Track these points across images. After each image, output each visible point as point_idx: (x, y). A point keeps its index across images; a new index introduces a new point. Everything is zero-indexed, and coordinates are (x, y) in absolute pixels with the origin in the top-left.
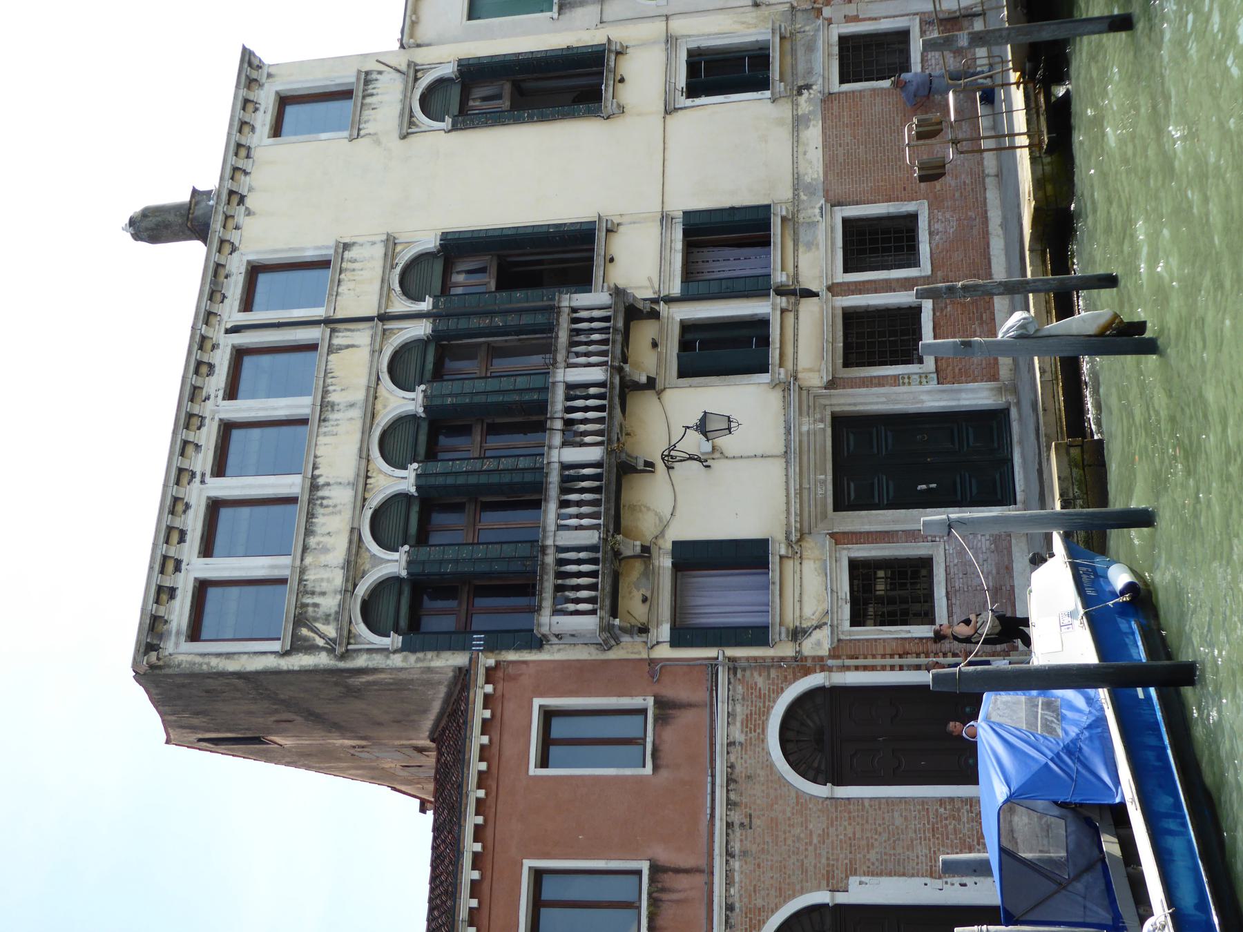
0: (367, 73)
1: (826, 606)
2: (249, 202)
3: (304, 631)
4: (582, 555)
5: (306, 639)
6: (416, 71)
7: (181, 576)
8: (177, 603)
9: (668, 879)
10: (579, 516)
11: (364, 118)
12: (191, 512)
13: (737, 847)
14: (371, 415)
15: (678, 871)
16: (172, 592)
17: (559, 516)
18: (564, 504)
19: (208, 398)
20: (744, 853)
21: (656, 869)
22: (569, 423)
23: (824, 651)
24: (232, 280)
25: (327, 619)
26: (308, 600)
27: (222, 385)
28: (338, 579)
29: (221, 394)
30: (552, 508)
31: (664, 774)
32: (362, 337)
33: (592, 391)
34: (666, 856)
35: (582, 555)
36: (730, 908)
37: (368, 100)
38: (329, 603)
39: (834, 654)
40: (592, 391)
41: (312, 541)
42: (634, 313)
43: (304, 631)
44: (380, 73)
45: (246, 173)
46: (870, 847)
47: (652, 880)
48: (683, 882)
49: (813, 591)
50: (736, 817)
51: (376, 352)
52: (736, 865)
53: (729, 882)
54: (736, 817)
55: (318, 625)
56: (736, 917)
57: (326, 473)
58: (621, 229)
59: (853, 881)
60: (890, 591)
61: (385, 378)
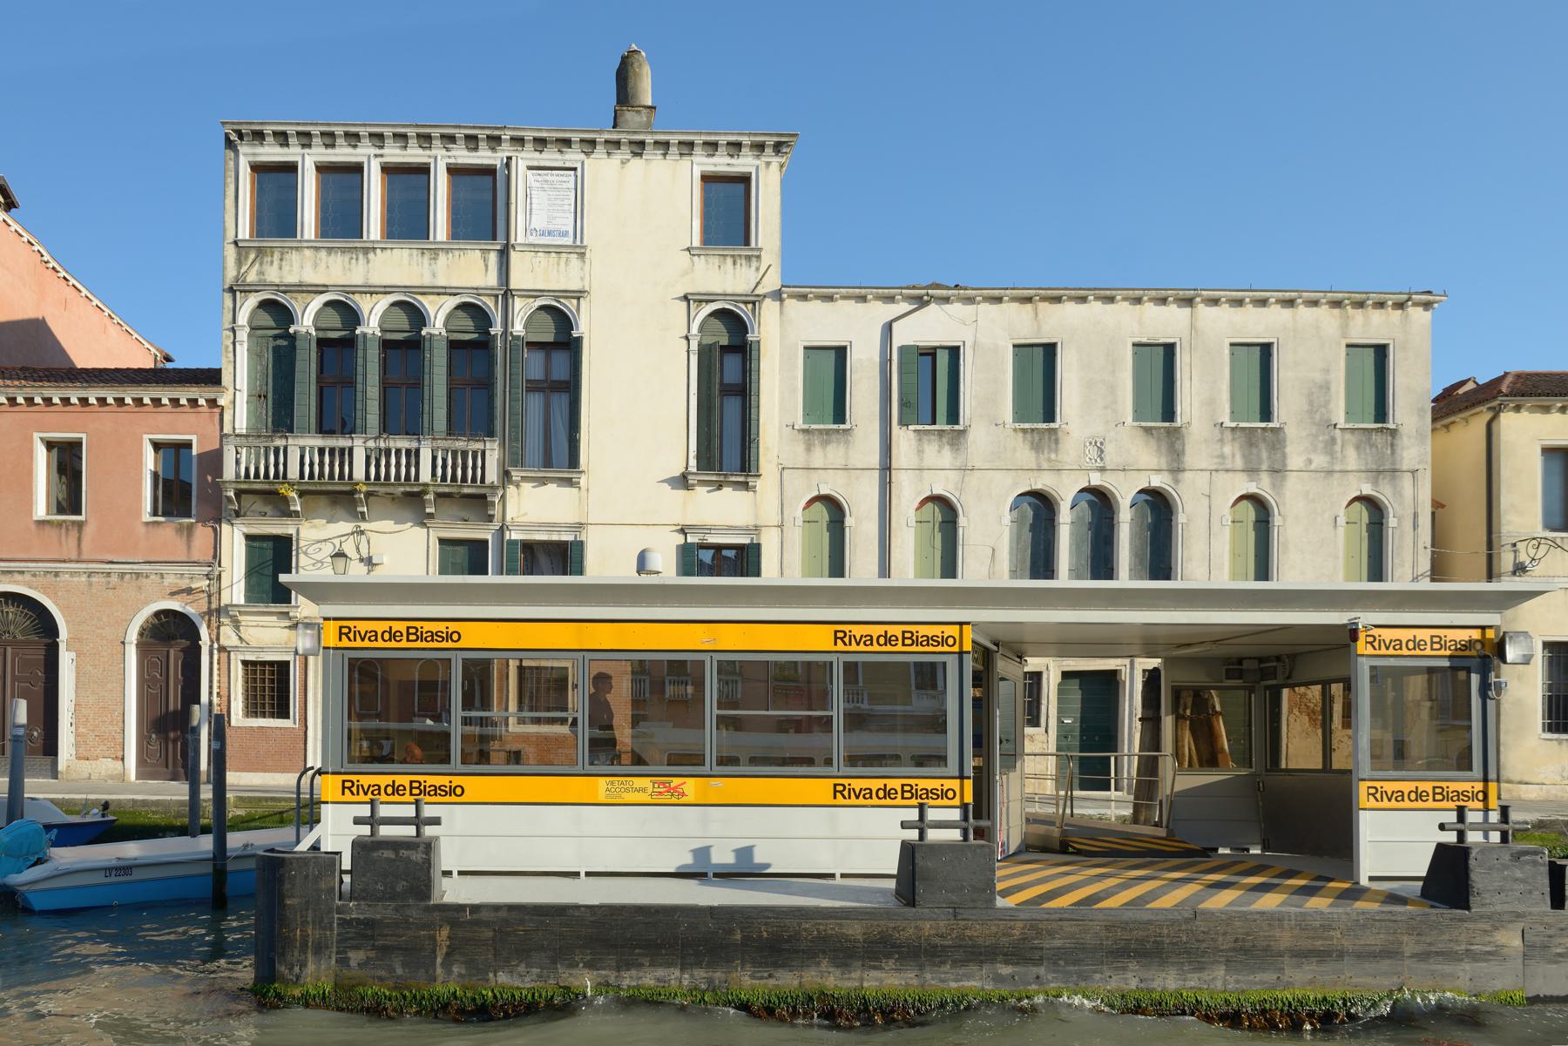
0: (758, 257)
1: (253, 644)
2: (636, 162)
3: (252, 256)
4: (281, 467)
5: (247, 257)
6: (754, 303)
7: (298, 150)
8: (278, 150)
9: (74, 533)
10: (312, 465)
11: (711, 259)
12: (350, 150)
13: (94, 579)
14: (426, 291)
15: (79, 539)
16: (285, 144)
17: (312, 448)
18: (321, 451)
19: (448, 150)
20: (90, 584)
21: (80, 525)
22: (388, 452)
23: (223, 642)
24: (558, 156)
25: (261, 273)
26: (277, 255)
27: (460, 161)
28: (291, 279)
29: (452, 161)
30: (318, 442)
31: (142, 530)
32: (492, 279)
33: (413, 470)
34: (88, 531)
35: (281, 467)
36: (57, 574)
37: (729, 261)
38: (273, 275)
39: (222, 649)
40: (413, 470)
41: (323, 253)
42: (479, 503)
43: (252, 256)
44: (758, 269)
45: (665, 155)
46: (95, 666)
47: (73, 522)
48: (73, 542)
49: (266, 635)
50: (114, 579)
51: (477, 291)
52: (84, 578)
53: (72, 574)
54: (114, 579)
55: (257, 266)
56: (51, 578)
57: (378, 258)
58: (575, 490)
59: (73, 655)
60: (271, 687)
61: (456, 300)
